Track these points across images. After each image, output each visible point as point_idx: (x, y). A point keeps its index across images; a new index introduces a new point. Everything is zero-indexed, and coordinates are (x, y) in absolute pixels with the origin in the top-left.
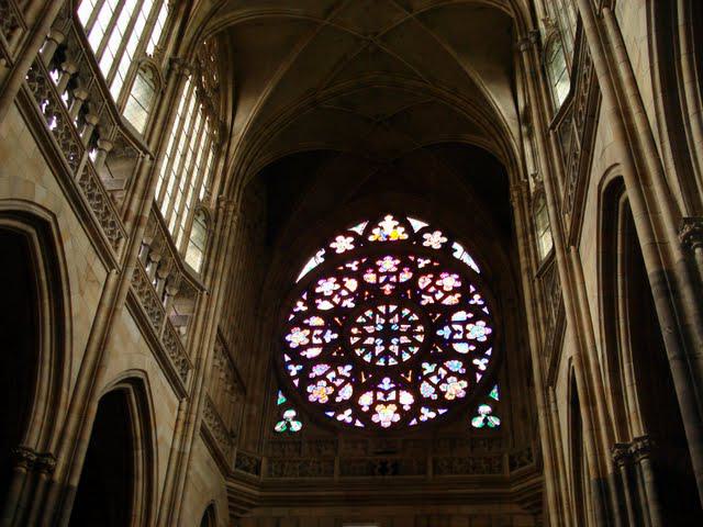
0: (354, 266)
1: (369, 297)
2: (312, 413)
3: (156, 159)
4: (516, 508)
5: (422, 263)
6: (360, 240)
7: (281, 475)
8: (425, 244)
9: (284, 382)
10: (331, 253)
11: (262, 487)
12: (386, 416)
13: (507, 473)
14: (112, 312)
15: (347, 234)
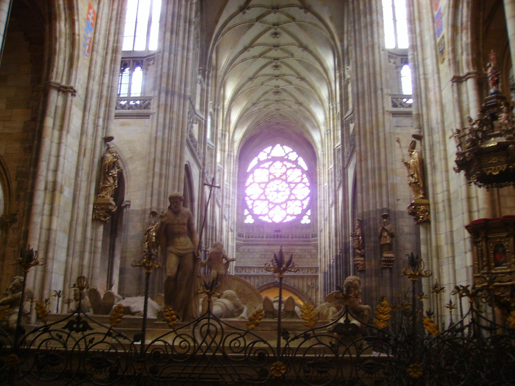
0: (266, 165)
1: (272, 178)
2: (255, 216)
3: (230, 187)
4: (312, 248)
5: (289, 165)
6: (269, 155)
7: (249, 237)
8: (289, 158)
9: (247, 207)
10: (259, 160)
11: (244, 241)
12: (277, 220)
13: (311, 239)
14: (228, 232)
15: (264, 152)
